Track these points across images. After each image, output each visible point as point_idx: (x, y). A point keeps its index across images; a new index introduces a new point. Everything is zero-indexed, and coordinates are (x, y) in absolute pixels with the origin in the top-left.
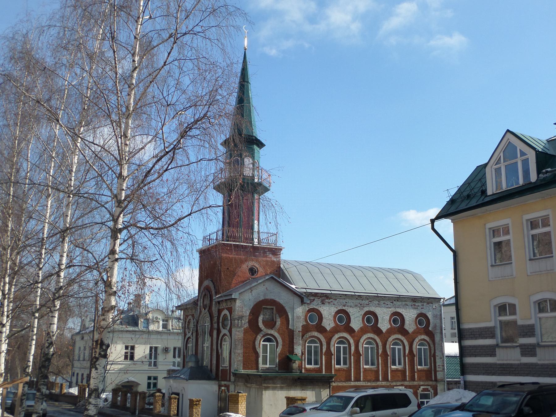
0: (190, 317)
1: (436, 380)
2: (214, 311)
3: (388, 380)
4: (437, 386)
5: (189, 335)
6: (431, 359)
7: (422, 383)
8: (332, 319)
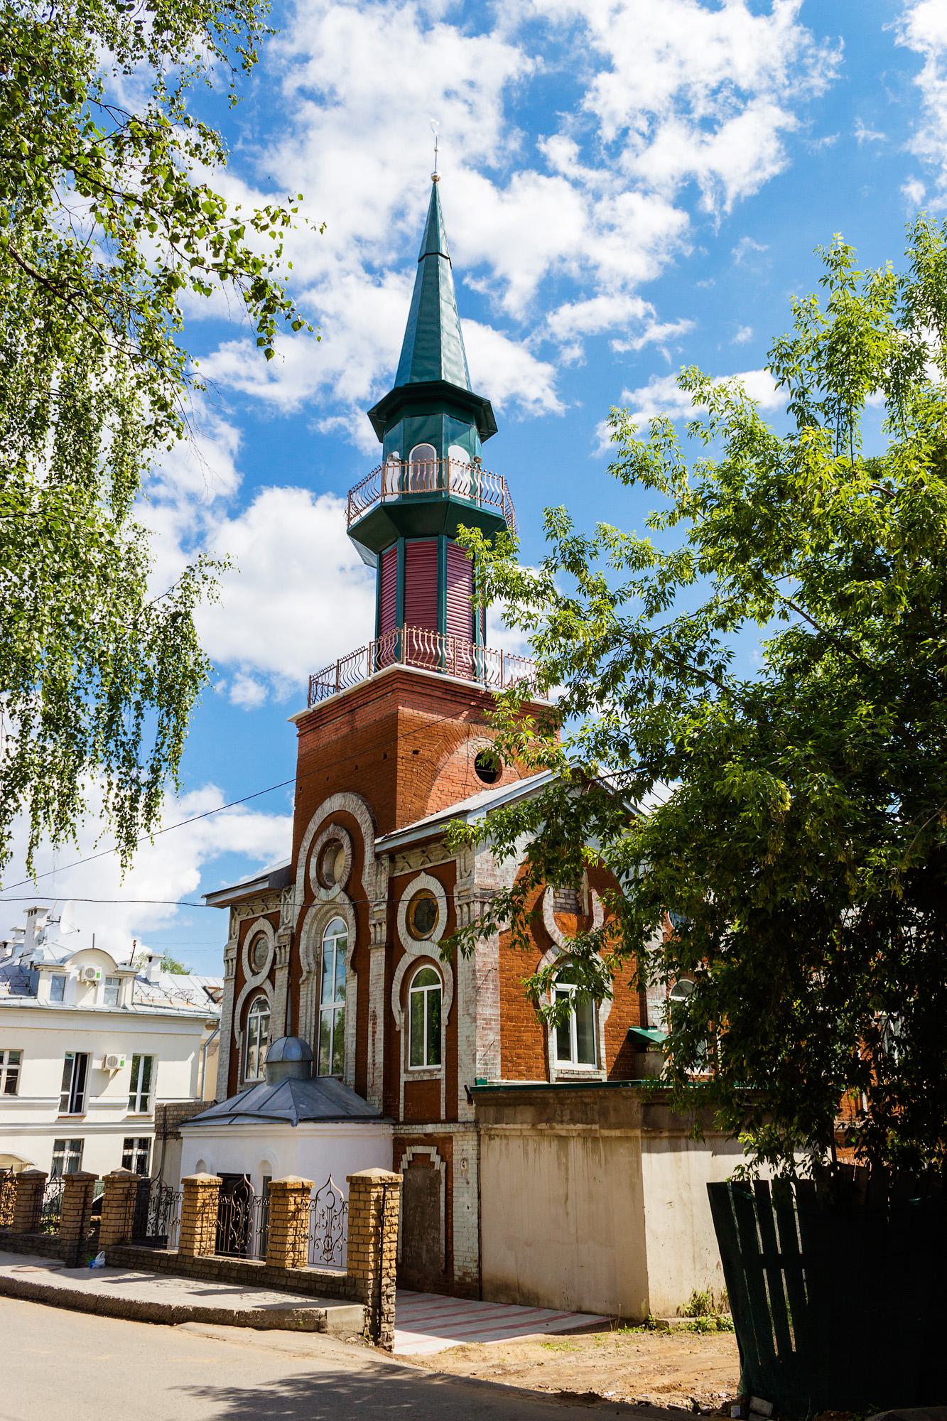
0: (264, 925)
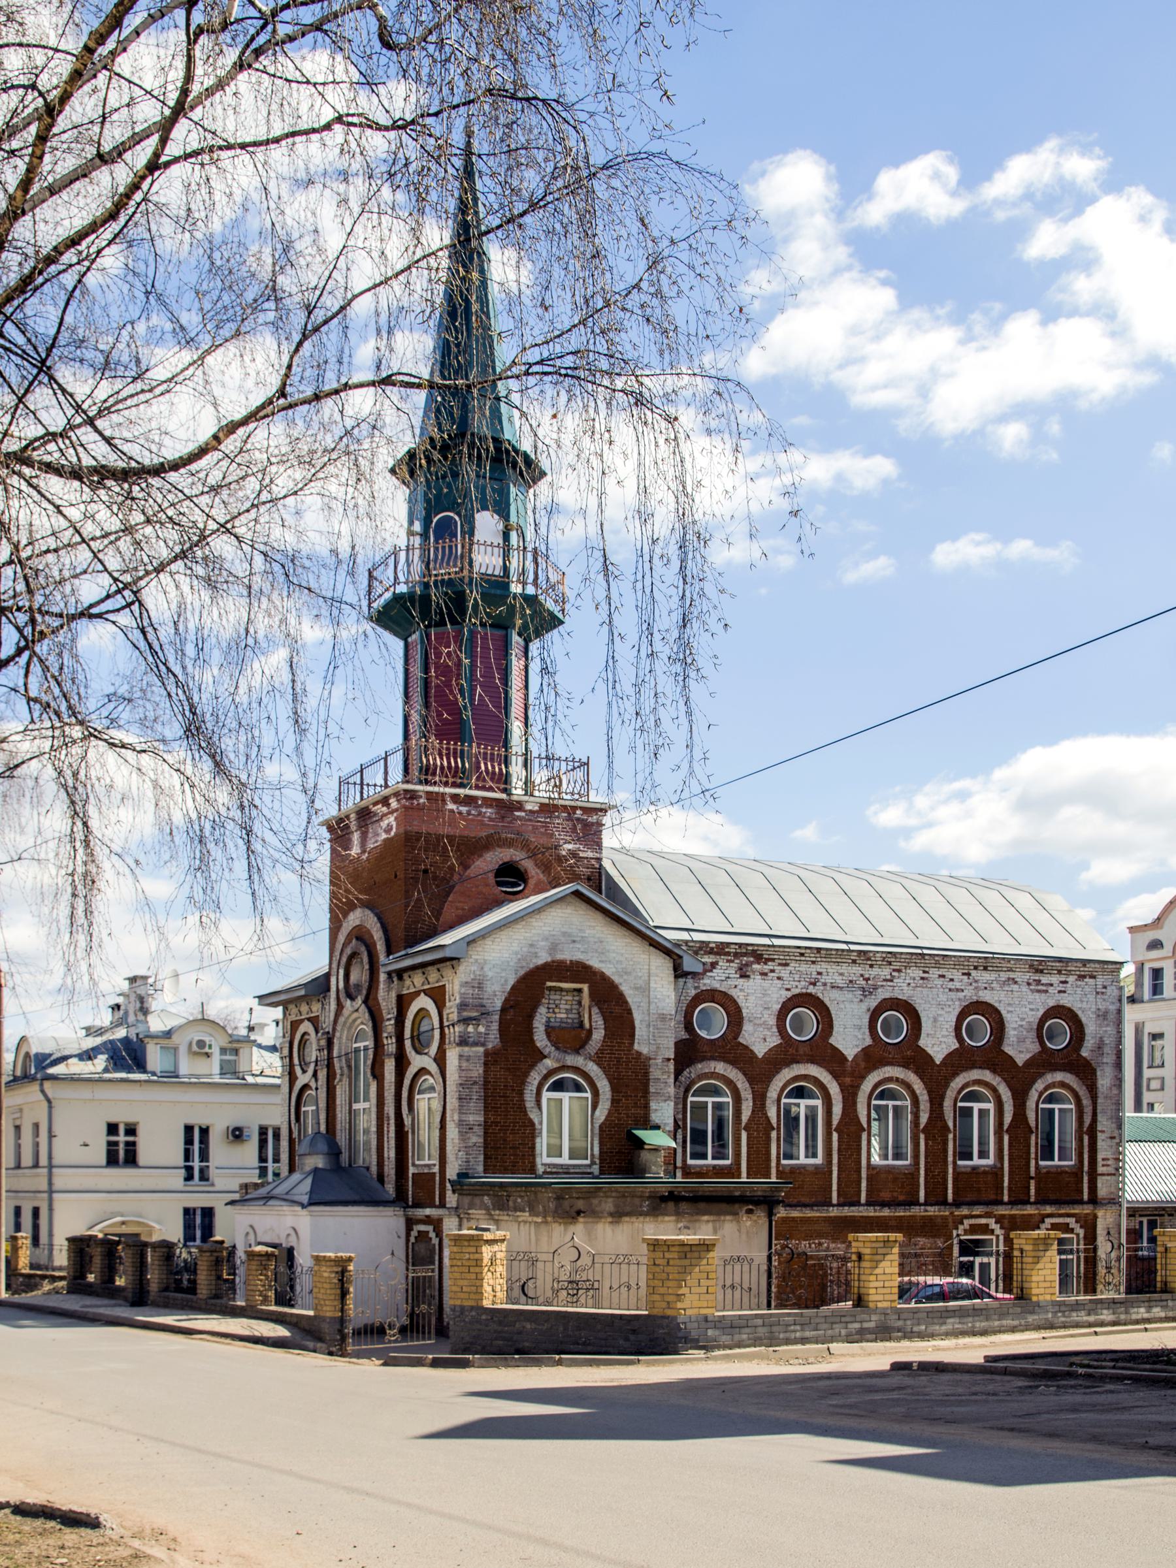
0: (307, 1027)
1: (1094, 1200)
2: (383, 1004)
3: (944, 1203)
4: (1095, 1217)
5: (303, 1079)
6: (1080, 1140)
7: (1049, 1209)
8: (772, 1021)
